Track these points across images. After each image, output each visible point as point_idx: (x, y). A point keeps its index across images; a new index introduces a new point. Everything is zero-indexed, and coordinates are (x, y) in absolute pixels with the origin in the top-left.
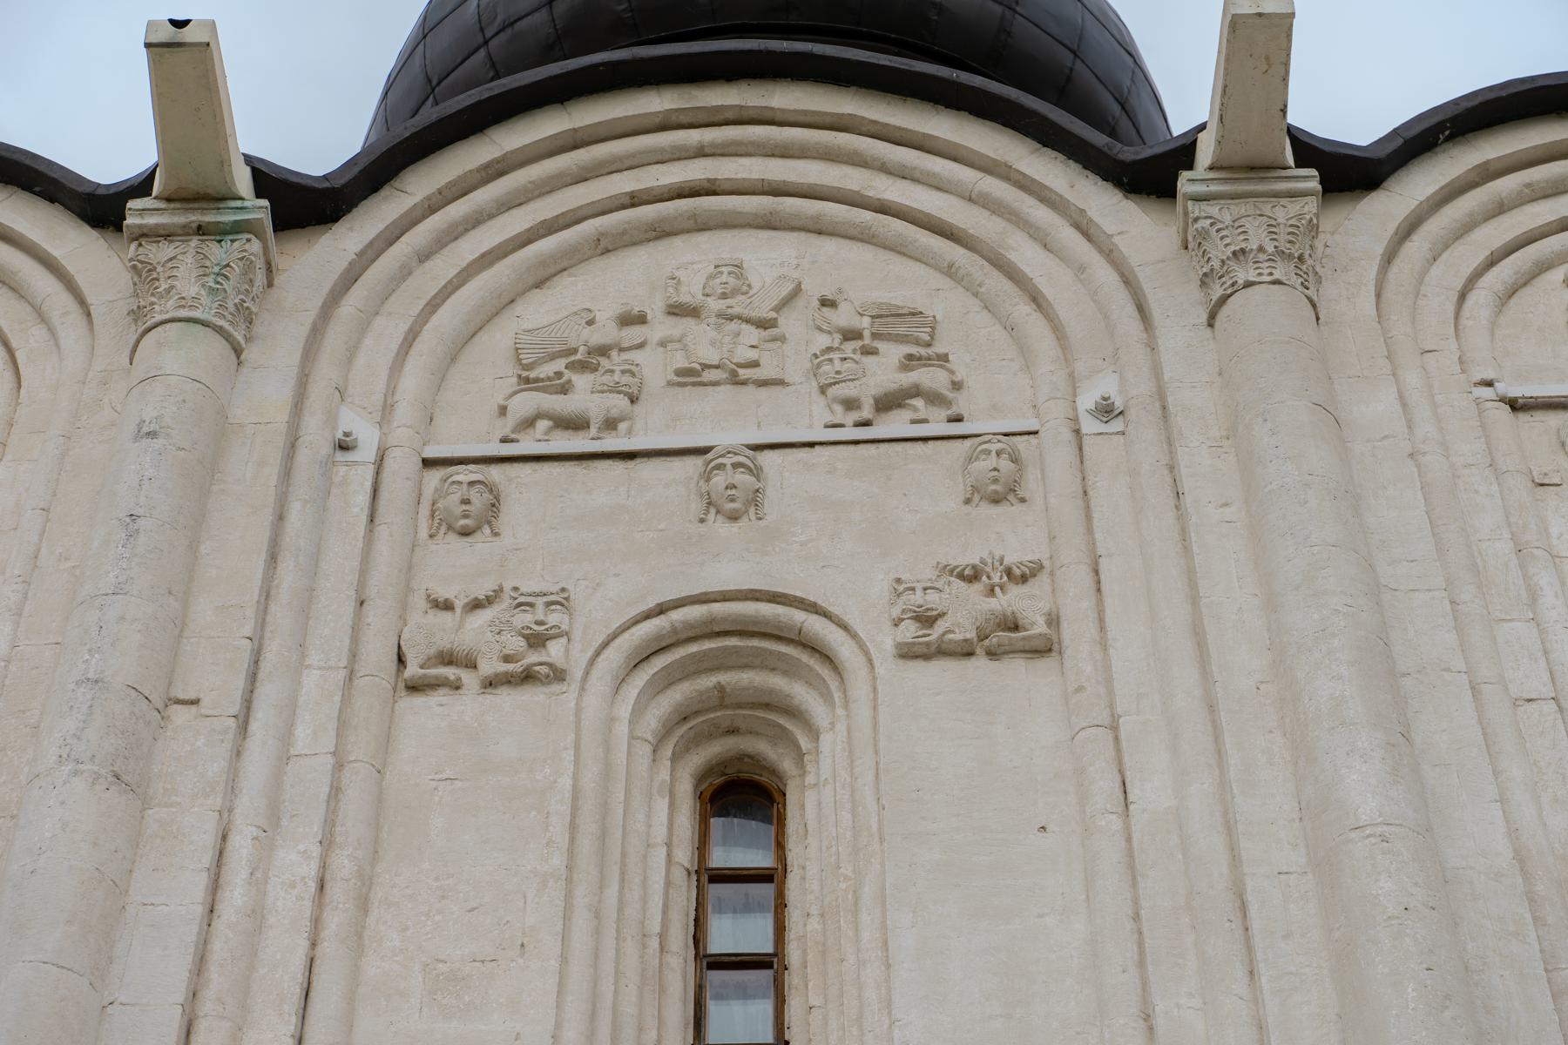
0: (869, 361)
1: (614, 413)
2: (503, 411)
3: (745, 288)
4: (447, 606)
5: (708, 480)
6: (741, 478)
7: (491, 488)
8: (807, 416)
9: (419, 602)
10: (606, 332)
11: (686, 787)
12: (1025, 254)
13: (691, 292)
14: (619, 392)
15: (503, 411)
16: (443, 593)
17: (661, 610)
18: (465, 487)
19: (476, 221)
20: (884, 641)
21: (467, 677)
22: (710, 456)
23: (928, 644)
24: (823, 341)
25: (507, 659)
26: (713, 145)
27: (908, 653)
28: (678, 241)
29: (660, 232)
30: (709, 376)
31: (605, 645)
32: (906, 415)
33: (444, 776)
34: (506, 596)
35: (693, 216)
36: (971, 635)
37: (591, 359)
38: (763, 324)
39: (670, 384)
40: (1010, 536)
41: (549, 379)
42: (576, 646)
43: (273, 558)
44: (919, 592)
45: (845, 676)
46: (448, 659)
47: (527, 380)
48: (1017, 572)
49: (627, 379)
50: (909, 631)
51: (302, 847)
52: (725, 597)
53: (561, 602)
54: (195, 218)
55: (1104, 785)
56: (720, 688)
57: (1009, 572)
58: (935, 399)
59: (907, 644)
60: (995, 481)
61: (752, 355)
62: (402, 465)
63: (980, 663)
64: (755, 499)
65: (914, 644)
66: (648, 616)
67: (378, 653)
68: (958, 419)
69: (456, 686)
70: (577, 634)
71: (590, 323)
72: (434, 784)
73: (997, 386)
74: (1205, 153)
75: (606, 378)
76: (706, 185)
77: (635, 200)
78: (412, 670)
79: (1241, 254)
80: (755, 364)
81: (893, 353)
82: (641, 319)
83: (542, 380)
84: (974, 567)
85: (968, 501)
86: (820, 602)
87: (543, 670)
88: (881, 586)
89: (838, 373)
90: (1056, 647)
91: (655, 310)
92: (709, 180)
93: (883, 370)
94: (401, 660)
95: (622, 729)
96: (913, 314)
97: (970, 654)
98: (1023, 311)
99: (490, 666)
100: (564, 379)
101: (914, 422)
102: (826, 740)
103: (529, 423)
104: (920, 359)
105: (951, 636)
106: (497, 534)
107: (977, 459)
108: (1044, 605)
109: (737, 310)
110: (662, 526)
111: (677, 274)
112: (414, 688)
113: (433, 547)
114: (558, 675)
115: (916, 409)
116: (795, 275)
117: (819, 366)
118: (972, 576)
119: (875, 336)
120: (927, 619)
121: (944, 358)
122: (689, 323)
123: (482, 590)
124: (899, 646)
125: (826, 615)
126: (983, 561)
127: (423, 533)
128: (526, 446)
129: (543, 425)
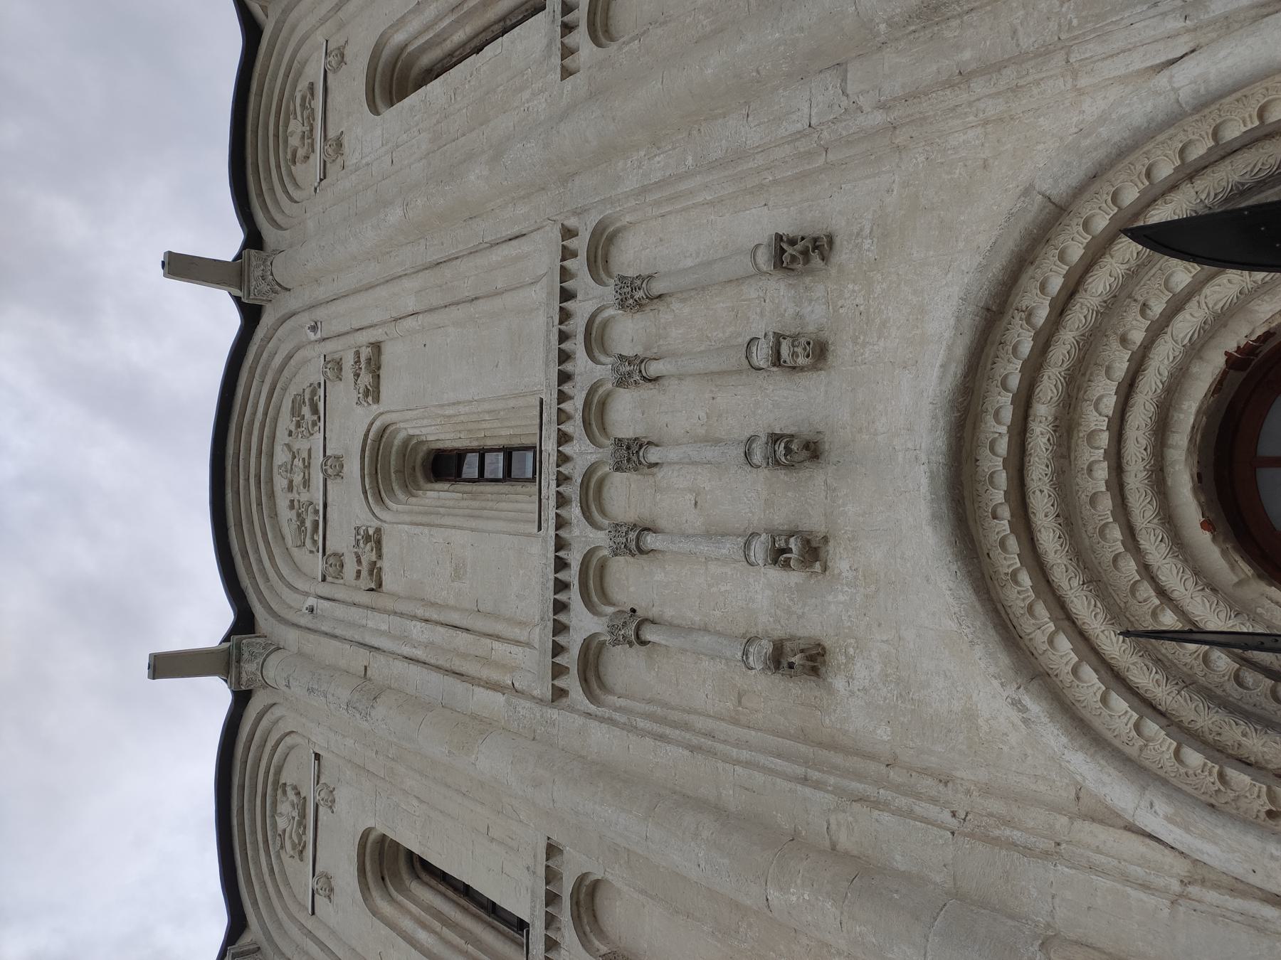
4: (359, 572)
11: (429, 486)
12: (277, 361)
13: (285, 483)
15: (311, 552)
17: (365, 492)
19: (260, 561)
27: (377, 400)
31: (373, 514)
38: (294, 457)
43: (335, 637)
46: (371, 573)
52: (362, 469)
53: (357, 529)
54: (234, 664)
55: (410, 323)
56: (396, 472)
58: (314, 393)
62: (324, 589)
63: (383, 373)
64: (337, 458)
66: (366, 498)
67: (366, 598)
73: (313, 373)
74: (238, 293)
77: (259, 504)
78: (373, 586)
79: (263, 278)
82: (292, 501)
88: (360, 410)
94: (372, 590)
102: (411, 432)
112: (380, 585)
114: (378, 531)
118: (357, 375)
125: (368, 431)
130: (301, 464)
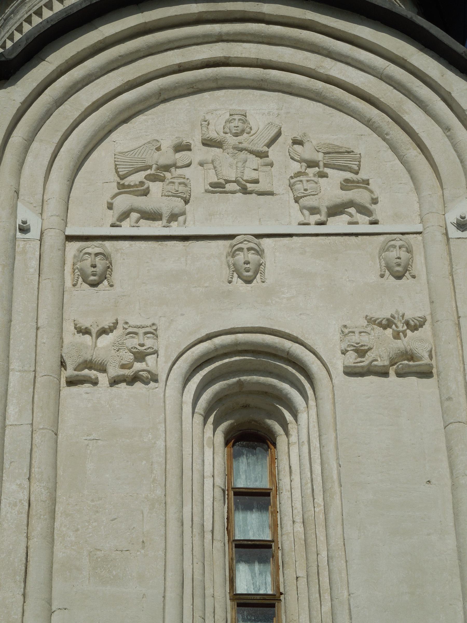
0: (322, 181)
1: (176, 211)
2: (110, 207)
3: (248, 130)
5: (233, 256)
6: (251, 257)
7: (105, 256)
8: (290, 218)
9: (69, 327)
10: (167, 156)
14: (178, 197)
16: (85, 323)
17: (209, 337)
18: (93, 256)
20: (338, 364)
21: (103, 379)
22: (234, 241)
23: (362, 367)
24: (296, 167)
25: (123, 367)
26: (228, 34)
27: (351, 372)
28: (206, 95)
29: (195, 89)
30: (229, 187)
32: (345, 218)
33: (92, 437)
34: (120, 326)
35: (215, 79)
36: (387, 363)
37: (160, 172)
39: (207, 191)
40: (408, 300)
41: (135, 186)
42: (162, 358)
44: (357, 334)
45: (315, 383)
46: (89, 364)
47: (123, 186)
48: (412, 323)
49: (181, 188)
50: (351, 359)
51: (18, 482)
57: (407, 323)
58: (363, 210)
59: (350, 367)
60: (399, 265)
61: (254, 175)
62: (53, 239)
65: (355, 367)
68: (375, 223)
69: (95, 383)
70: (161, 352)
71: (158, 149)
72: (86, 442)
73: (398, 202)
75: (170, 187)
76: (223, 60)
80: (256, 182)
81: (337, 176)
82: (188, 148)
83: (132, 187)
84: (388, 320)
85: (382, 276)
86: (299, 337)
87: (145, 374)
89: (306, 190)
90: (434, 371)
91: (195, 141)
92: (225, 57)
93: (330, 189)
94: (63, 364)
95: (187, 408)
96: (348, 152)
97: (385, 374)
98: (413, 153)
99: (114, 371)
100: (146, 186)
101: (350, 223)
102: (303, 417)
103: (125, 215)
104: (353, 182)
105: (375, 363)
106: (112, 286)
107: (388, 250)
108: (427, 346)
109: (245, 145)
110: (207, 285)
111: (207, 118)
112: (71, 383)
113: (75, 293)
115: (351, 215)
116: (277, 122)
117: (294, 184)
118: (387, 324)
119: (326, 165)
120: (361, 352)
121: (367, 182)
122: (217, 151)
123: (106, 323)
124: (345, 367)
126: (392, 316)
127: (68, 283)
128: (126, 229)
129: (135, 216)
130: (250, 174)
